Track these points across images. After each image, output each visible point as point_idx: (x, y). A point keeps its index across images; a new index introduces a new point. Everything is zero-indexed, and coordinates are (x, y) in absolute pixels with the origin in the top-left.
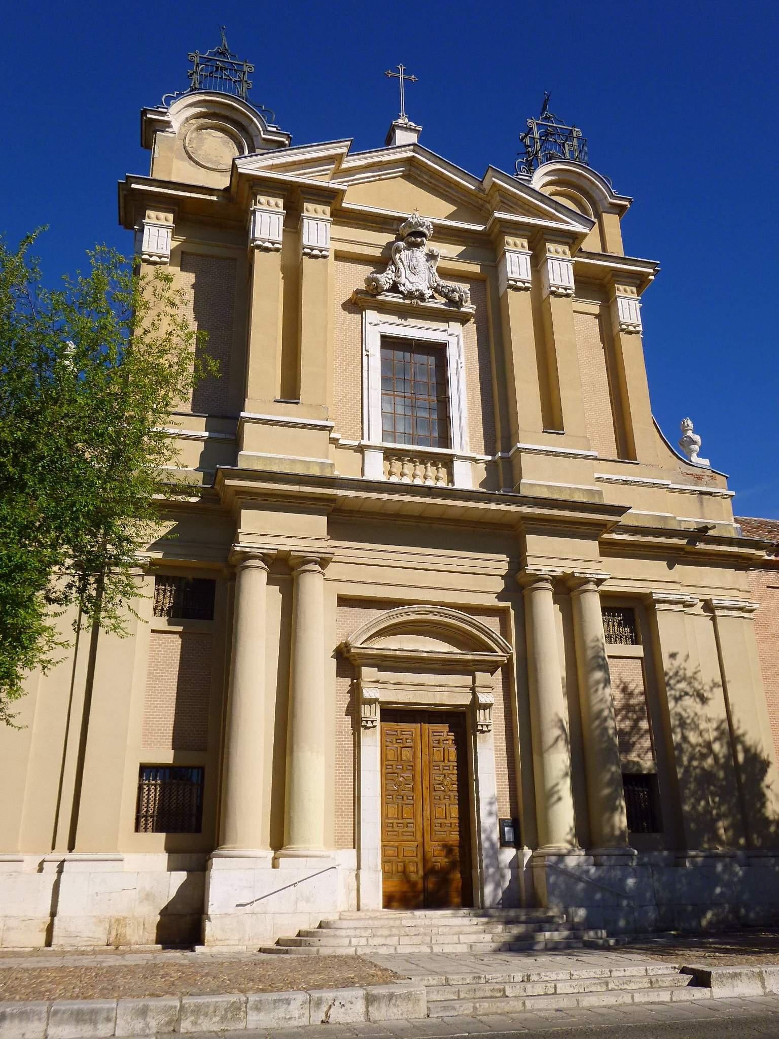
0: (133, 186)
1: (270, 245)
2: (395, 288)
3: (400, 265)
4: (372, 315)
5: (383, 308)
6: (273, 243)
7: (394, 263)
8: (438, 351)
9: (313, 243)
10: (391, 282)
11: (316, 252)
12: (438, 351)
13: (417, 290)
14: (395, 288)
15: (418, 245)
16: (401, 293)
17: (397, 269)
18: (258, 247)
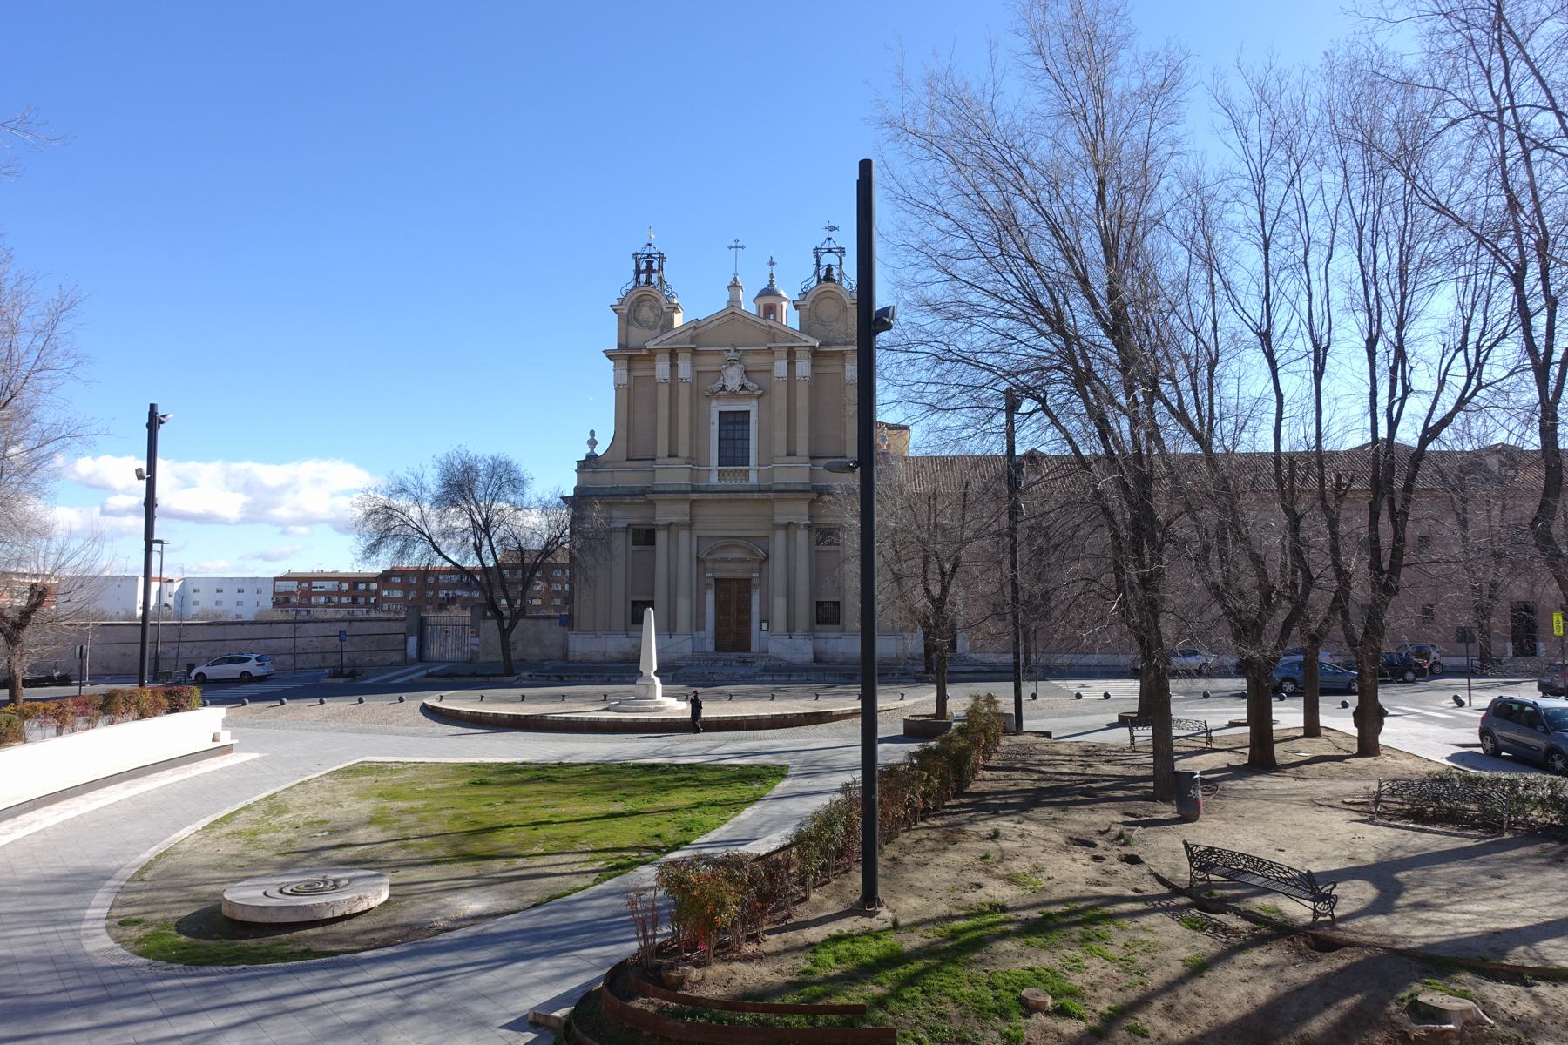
2: (723, 388)
4: (714, 403)
5: (718, 398)
8: (748, 412)
12: (748, 412)
14: (723, 388)
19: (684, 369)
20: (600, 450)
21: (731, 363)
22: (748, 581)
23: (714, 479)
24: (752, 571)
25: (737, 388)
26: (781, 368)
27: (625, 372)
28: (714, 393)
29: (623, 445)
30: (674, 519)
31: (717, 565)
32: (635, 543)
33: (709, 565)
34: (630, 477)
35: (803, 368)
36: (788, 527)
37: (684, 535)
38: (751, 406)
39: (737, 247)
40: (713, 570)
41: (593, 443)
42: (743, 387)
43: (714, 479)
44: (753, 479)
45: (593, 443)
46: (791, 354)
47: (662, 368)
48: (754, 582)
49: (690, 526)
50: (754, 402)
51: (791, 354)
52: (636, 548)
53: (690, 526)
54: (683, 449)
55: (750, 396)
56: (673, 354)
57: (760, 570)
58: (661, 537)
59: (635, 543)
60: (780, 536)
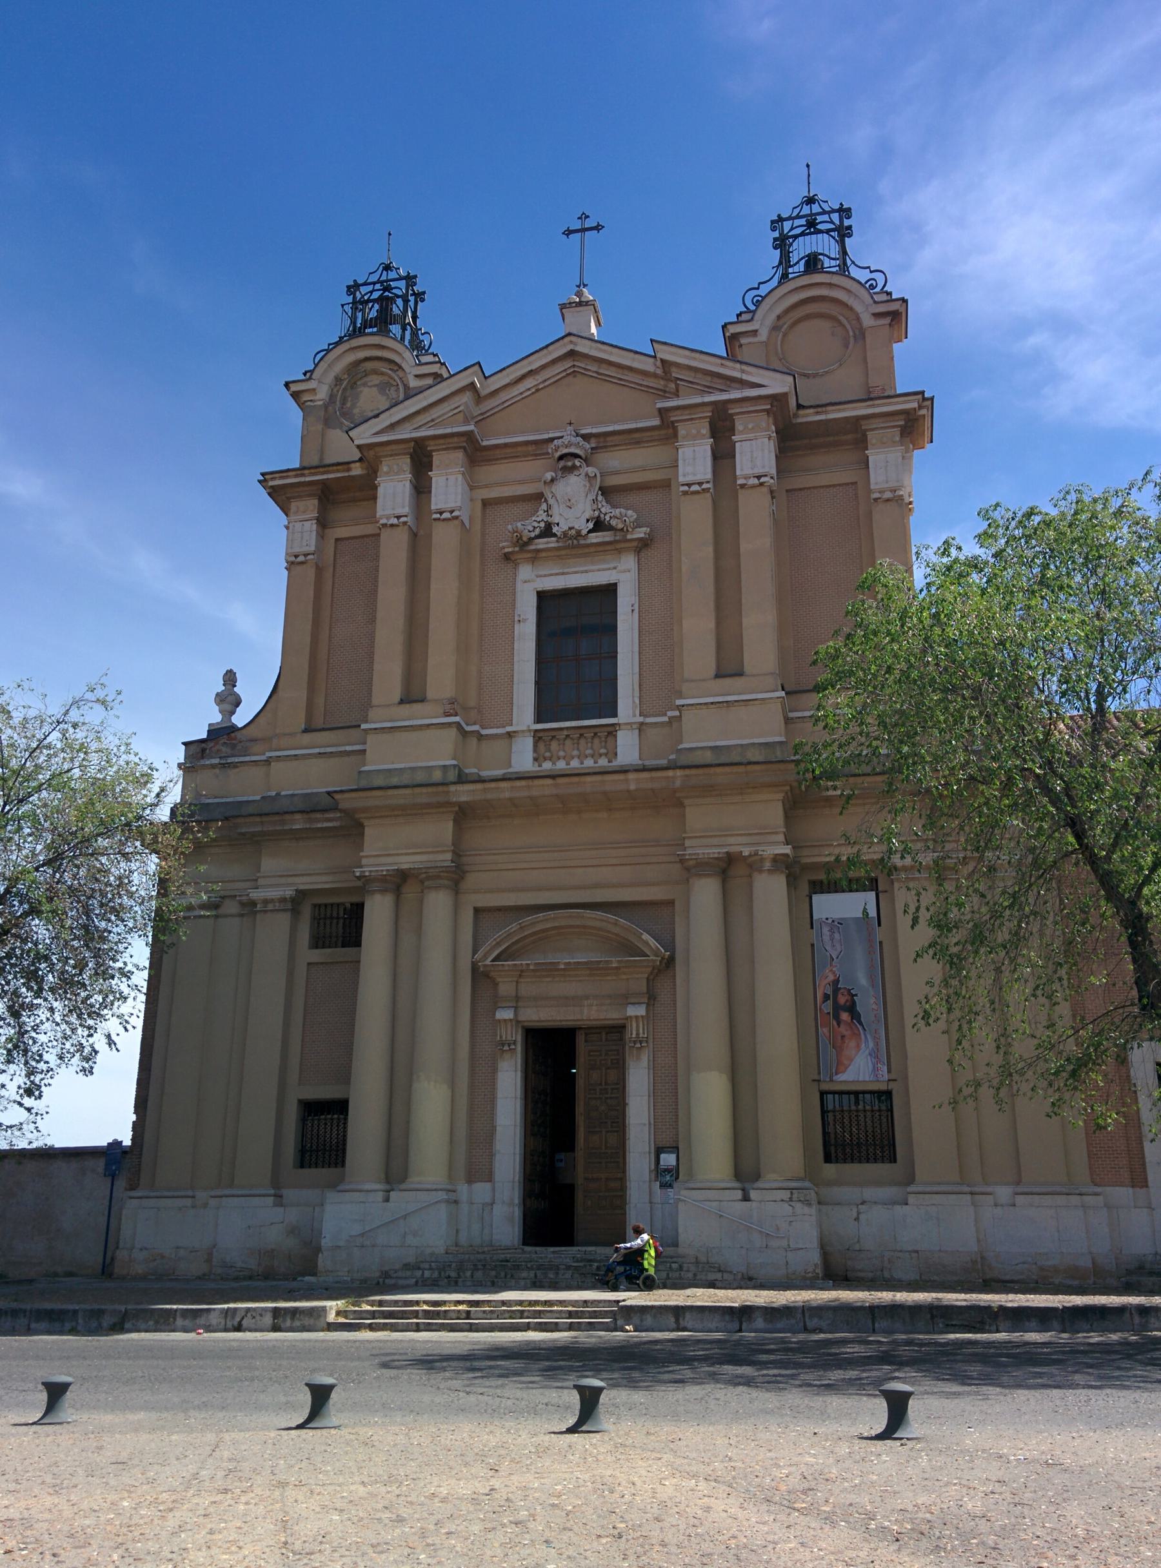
0: (271, 483)
1: (395, 521)
2: (547, 531)
3: (551, 501)
4: (525, 571)
5: (536, 558)
6: (398, 517)
7: (546, 501)
8: (609, 591)
9: (441, 506)
10: (542, 525)
11: (446, 515)
12: (609, 591)
13: (570, 529)
14: (547, 531)
15: (574, 467)
16: (555, 535)
17: (549, 507)
18: (384, 525)
19: (449, 488)
20: (240, 719)
21: (567, 463)
22: (618, 1029)
23: (523, 758)
24: (626, 999)
25: (585, 527)
26: (695, 460)
27: (311, 527)
28: (523, 544)
29: (297, 695)
30: (406, 862)
31: (528, 988)
32: (318, 942)
33: (506, 988)
34: (305, 773)
35: (756, 454)
36: (728, 868)
37: (438, 903)
38: (623, 574)
39: (585, 228)
40: (517, 1001)
41: (229, 700)
42: (599, 525)
43: (523, 758)
44: (628, 749)
45: (229, 700)
46: (722, 429)
47: (394, 493)
48: (633, 1031)
49: (455, 877)
50: (629, 562)
51: (722, 429)
52: (317, 955)
53: (455, 877)
54: (441, 679)
55: (615, 548)
56: (421, 459)
57: (651, 998)
58: (378, 913)
59: (318, 942)
60: (706, 894)
